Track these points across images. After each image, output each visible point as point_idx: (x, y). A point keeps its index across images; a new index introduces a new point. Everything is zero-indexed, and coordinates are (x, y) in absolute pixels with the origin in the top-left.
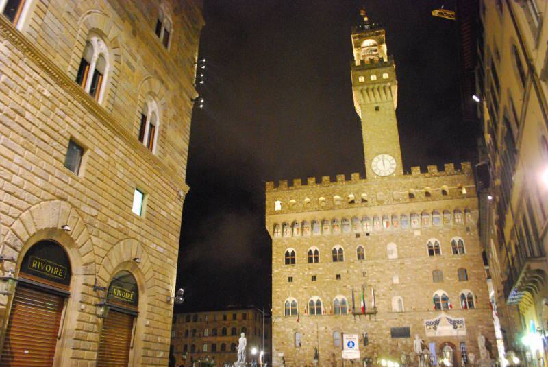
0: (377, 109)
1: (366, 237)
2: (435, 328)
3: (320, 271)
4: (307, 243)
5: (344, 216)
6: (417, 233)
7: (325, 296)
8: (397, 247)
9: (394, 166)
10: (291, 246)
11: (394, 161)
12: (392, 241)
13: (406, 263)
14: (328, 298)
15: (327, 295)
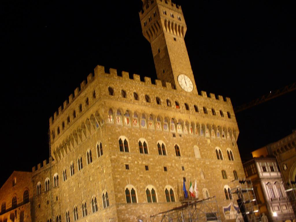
0: (175, 39)
1: (180, 137)
2: (229, 213)
3: (151, 162)
4: (137, 134)
5: (166, 116)
6: (209, 141)
7: (158, 185)
8: (200, 150)
9: (192, 86)
10: (123, 134)
11: (191, 83)
12: (196, 144)
13: (206, 163)
14: (161, 187)
15: (160, 185)
